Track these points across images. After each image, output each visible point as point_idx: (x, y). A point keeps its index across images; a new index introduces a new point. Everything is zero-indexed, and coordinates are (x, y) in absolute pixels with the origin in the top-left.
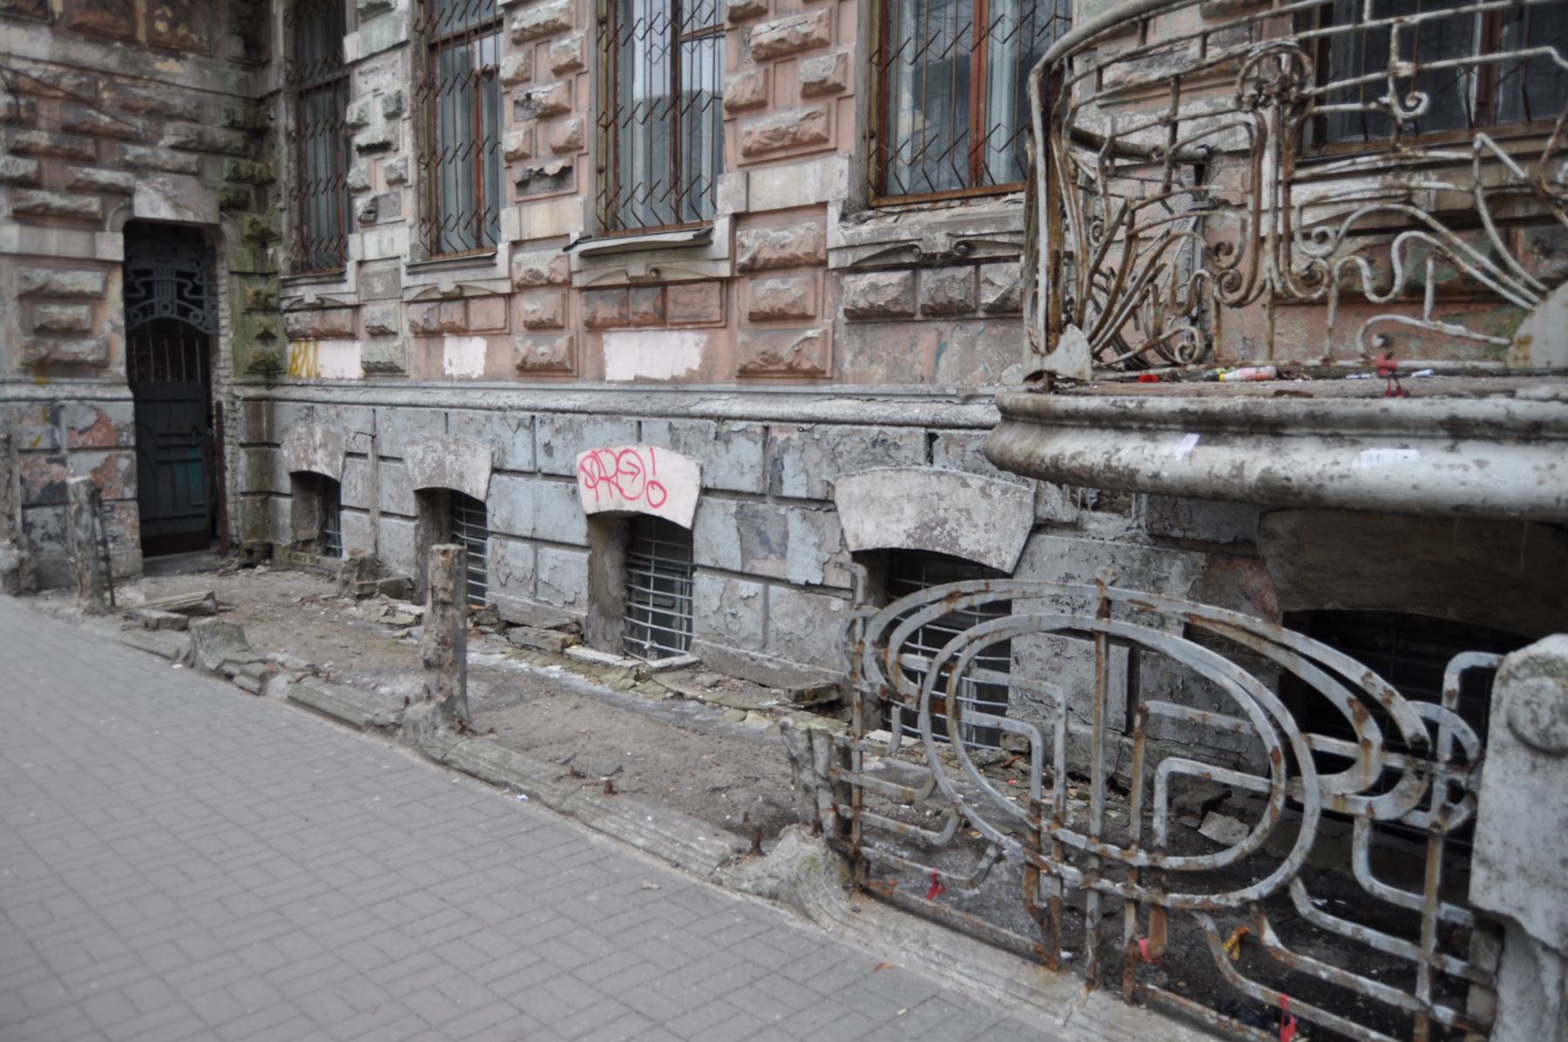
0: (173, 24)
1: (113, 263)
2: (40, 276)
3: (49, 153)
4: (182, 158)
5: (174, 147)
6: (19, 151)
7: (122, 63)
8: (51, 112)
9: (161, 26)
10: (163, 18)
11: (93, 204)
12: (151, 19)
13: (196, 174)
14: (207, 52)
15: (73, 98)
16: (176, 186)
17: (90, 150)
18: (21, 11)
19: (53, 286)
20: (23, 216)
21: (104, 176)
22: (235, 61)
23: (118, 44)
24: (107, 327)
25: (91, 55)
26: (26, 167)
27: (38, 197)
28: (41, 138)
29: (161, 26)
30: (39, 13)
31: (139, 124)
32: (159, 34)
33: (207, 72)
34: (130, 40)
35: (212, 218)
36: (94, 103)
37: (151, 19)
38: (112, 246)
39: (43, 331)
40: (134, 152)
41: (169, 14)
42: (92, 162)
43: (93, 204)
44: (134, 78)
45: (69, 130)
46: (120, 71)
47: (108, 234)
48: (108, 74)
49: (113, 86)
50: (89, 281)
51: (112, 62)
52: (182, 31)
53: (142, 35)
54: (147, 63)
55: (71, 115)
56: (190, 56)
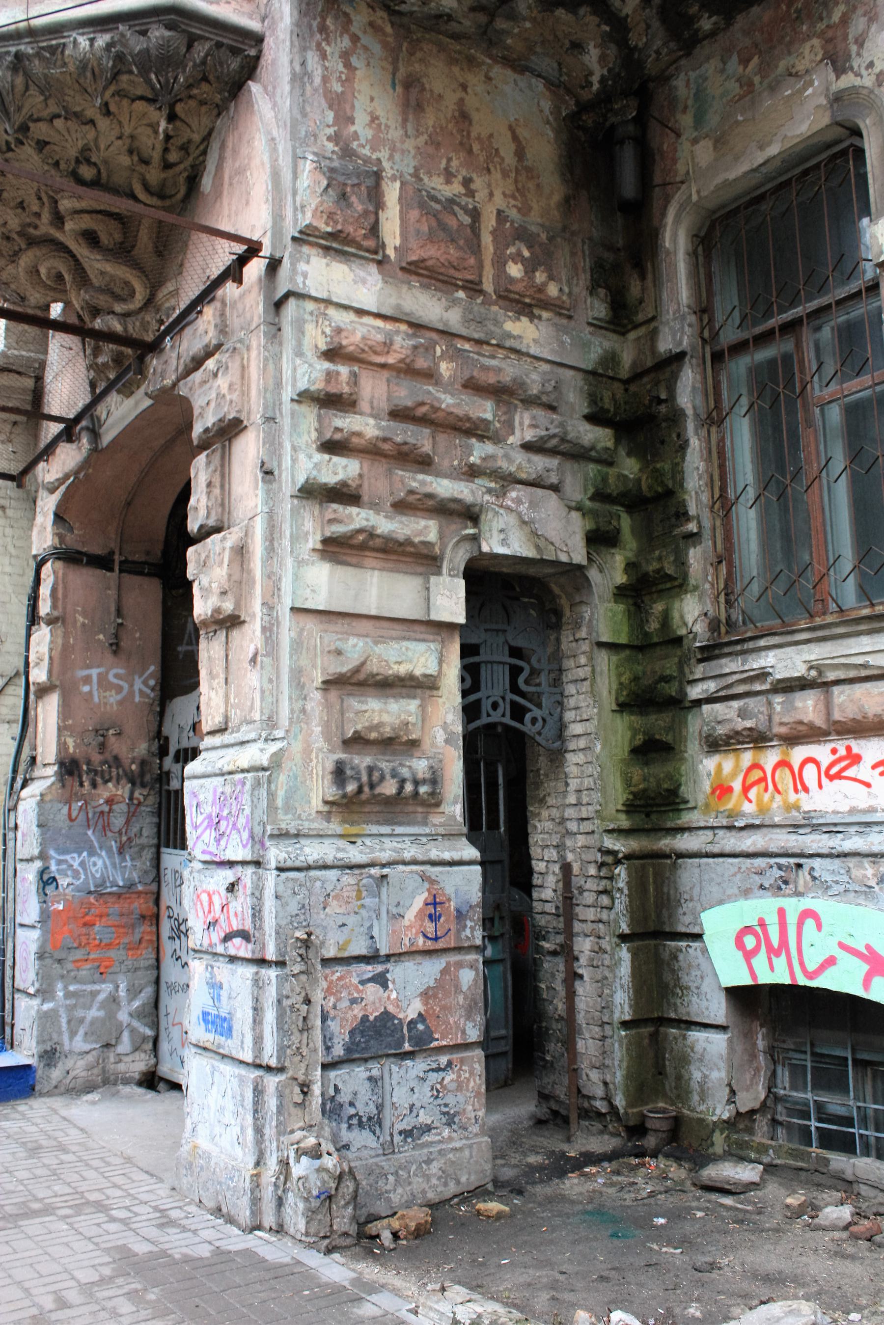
0: (530, 268)
1: (450, 627)
2: (356, 649)
3: (372, 451)
4: (539, 464)
5: (527, 447)
6: (333, 446)
7: (466, 321)
8: (374, 389)
9: (515, 270)
10: (517, 258)
11: (425, 529)
12: (500, 263)
13: (555, 488)
14: (562, 311)
15: (406, 370)
16: (533, 505)
17: (427, 447)
18: (348, 240)
19: (373, 667)
20: (337, 548)
21: (445, 487)
22: (596, 326)
23: (461, 294)
24: (440, 736)
25: (429, 306)
26: (340, 470)
27: (357, 518)
28: (364, 425)
29: (515, 270)
30: (370, 243)
31: (485, 410)
32: (512, 280)
33: (567, 339)
34: (474, 288)
35: (579, 556)
36: (430, 375)
37: (500, 263)
38: (450, 601)
39: (356, 741)
40: (479, 452)
41: (526, 254)
42: (424, 463)
43: (425, 529)
44: (479, 342)
45: (398, 414)
46: (464, 332)
47: (445, 579)
48: (446, 334)
49: (456, 355)
50: (419, 657)
51: (454, 319)
52: (540, 277)
53: (488, 286)
54: (496, 323)
55: (405, 394)
56: (545, 315)
